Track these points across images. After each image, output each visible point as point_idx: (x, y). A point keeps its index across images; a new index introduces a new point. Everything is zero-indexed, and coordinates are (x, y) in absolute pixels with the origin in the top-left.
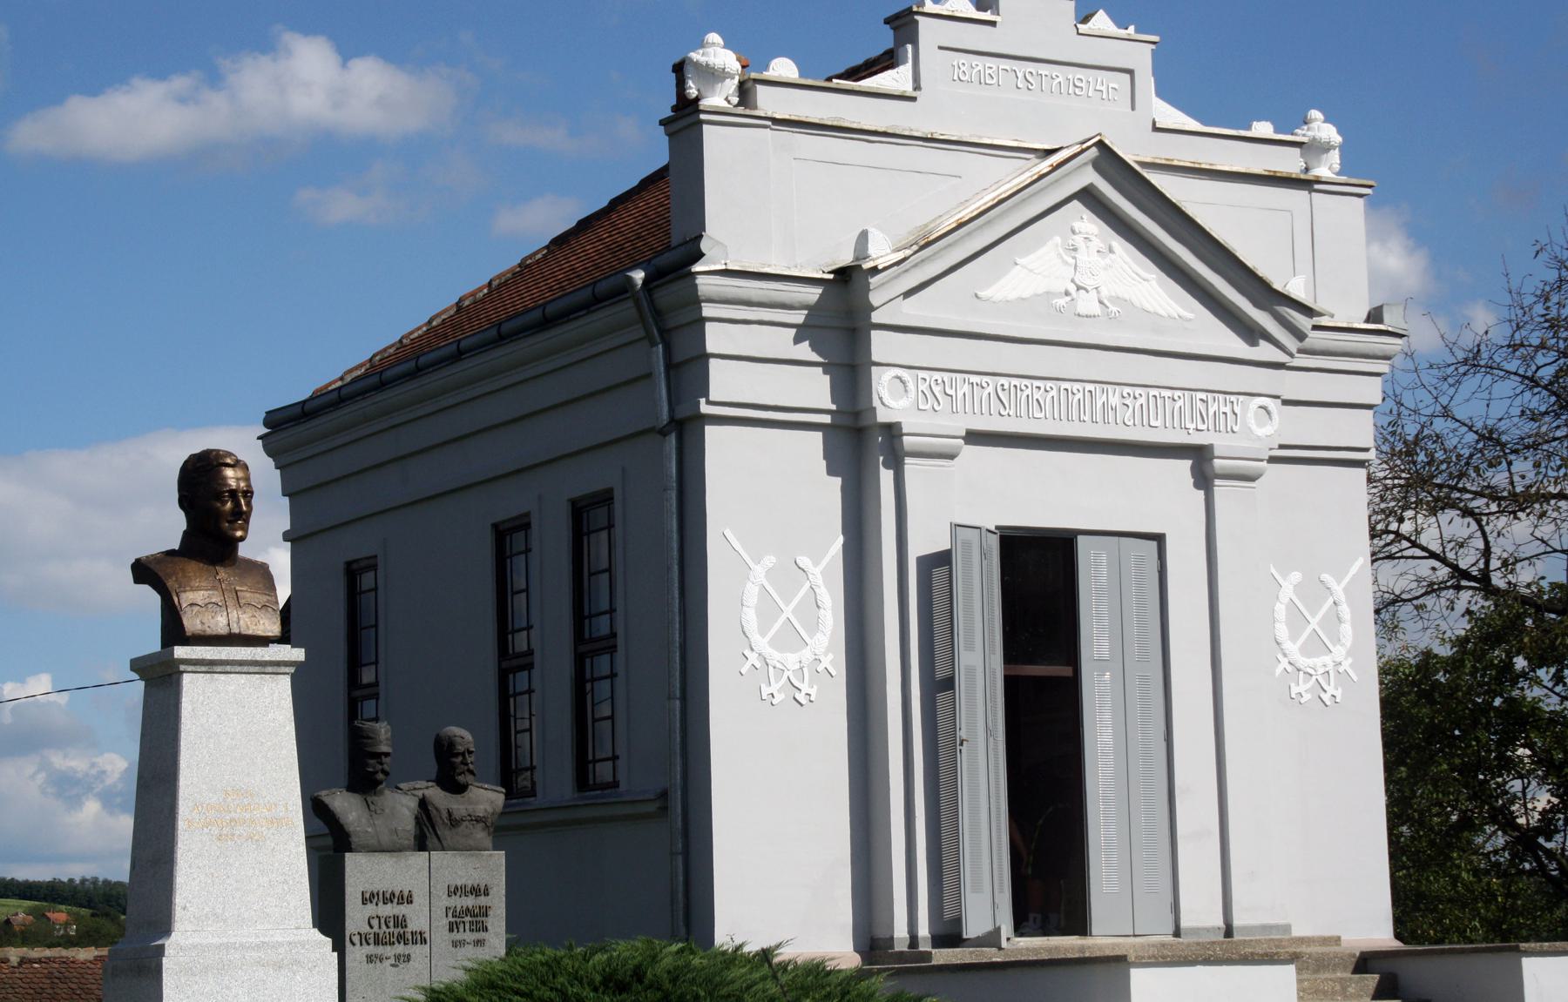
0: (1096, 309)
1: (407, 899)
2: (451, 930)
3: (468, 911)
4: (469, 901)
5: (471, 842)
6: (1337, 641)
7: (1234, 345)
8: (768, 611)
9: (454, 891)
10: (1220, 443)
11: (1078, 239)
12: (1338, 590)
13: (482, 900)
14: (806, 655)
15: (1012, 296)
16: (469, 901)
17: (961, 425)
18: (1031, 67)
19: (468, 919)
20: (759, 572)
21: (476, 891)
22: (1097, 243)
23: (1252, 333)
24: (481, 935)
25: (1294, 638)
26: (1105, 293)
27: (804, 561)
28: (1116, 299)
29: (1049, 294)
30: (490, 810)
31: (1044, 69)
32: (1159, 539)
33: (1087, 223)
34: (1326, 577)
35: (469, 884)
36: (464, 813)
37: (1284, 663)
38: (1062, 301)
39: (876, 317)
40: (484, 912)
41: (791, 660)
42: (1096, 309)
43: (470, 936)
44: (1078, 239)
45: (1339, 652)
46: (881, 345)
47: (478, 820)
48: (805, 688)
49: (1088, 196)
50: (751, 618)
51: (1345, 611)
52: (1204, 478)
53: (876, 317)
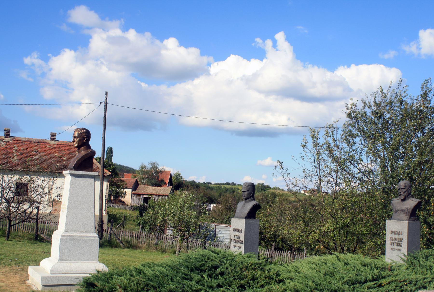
1: (240, 231)
2: (391, 245)
3: (396, 239)
4: (396, 236)
5: (399, 218)
9: (392, 232)
13: (400, 237)
16: (396, 236)
19: (396, 242)
21: (399, 233)
24: (399, 248)
30: (409, 208)
35: (397, 230)
36: (399, 208)
40: (401, 240)
43: (396, 247)
47: (402, 211)
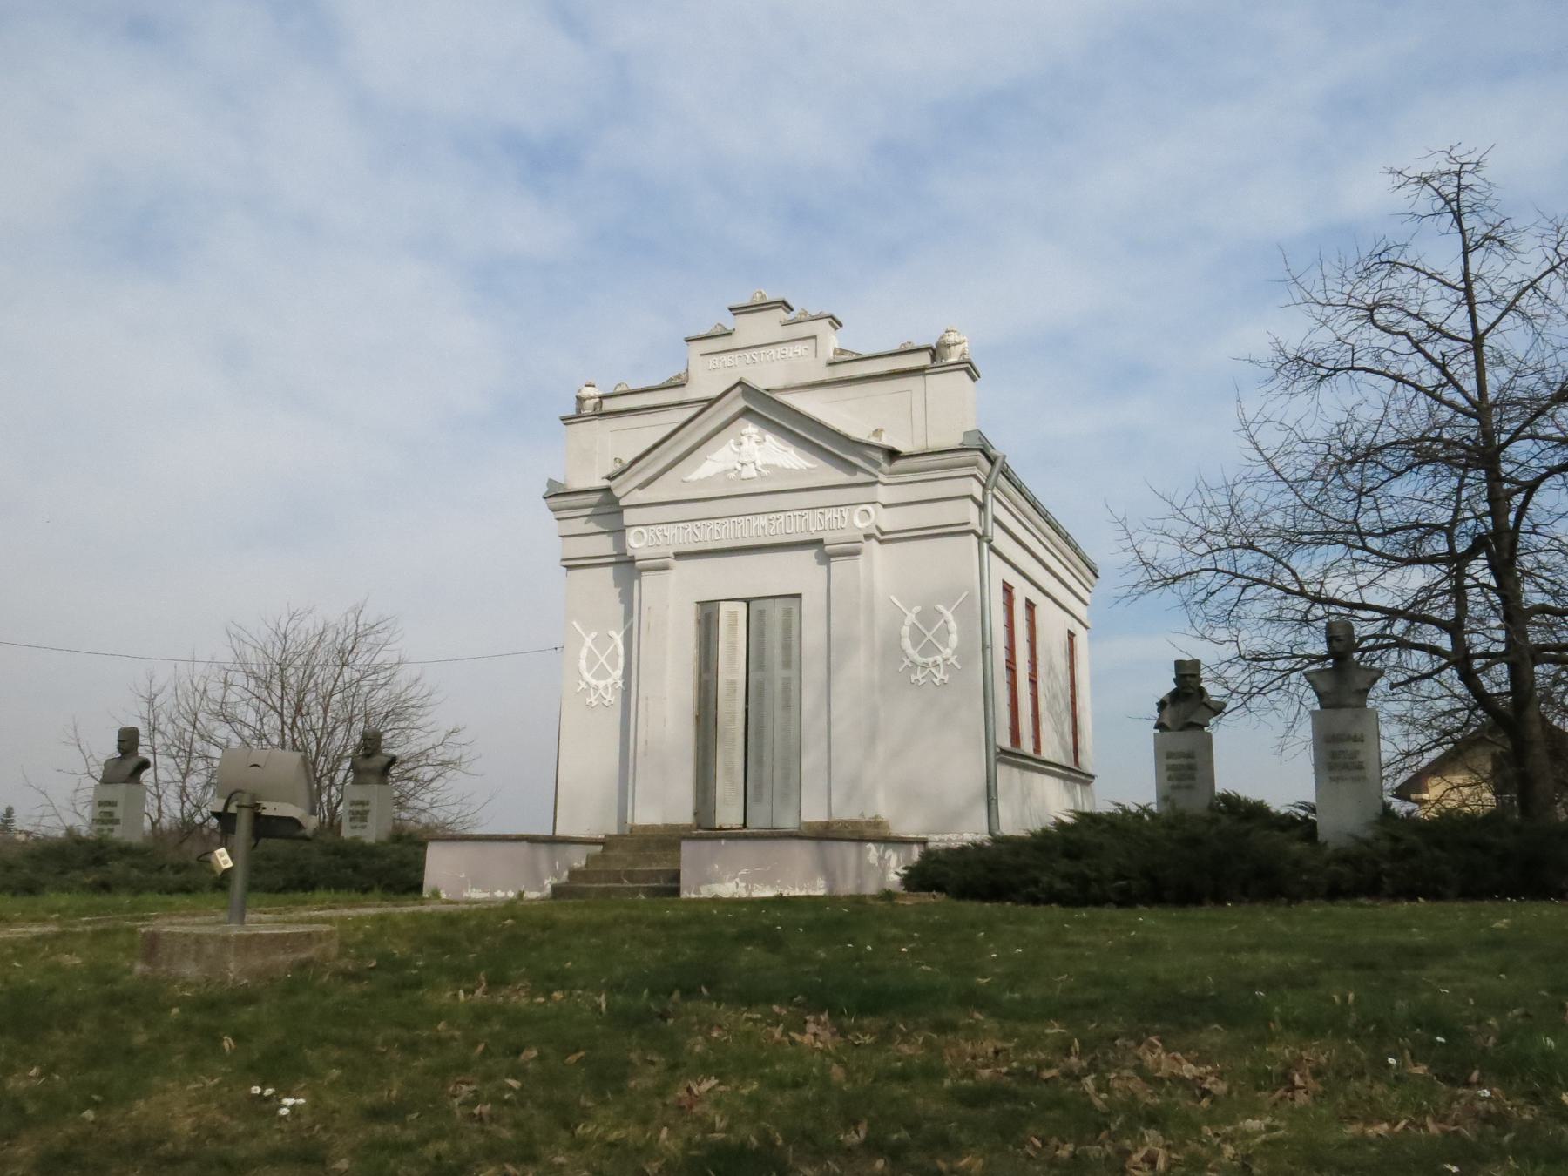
0: (755, 474)
4: (359, 808)
6: (946, 646)
7: (841, 477)
8: (592, 660)
9: (353, 803)
10: (827, 537)
11: (744, 439)
12: (949, 615)
14: (610, 681)
15: (703, 476)
16: (359, 808)
17: (671, 552)
18: (756, 351)
20: (588, 642)
21: (362, 803)
22: (756, 437)
23: (852, 468)
25: (915, 646)
26: (759, 463)
27: (612, 633)
28: (766, 466)
29: (726, 471)
31: (762, 350)
32: (799, 596)
33: (751, 429)
34: (941, 607)
37: (907, 662)
38: (732, 475)
39: (622, 503)
40: (367, 812)
41: (601, 684)
42: (755, 474)
44: (744, 439)
45: (948, 652)
46: (629, 517)
48: (608, 697)
49: (746, 412)
50: (583, 664)
51: (953, 626)
52: (826, 558)
53: (622, 503)
